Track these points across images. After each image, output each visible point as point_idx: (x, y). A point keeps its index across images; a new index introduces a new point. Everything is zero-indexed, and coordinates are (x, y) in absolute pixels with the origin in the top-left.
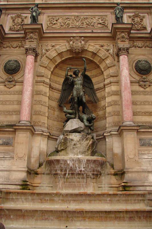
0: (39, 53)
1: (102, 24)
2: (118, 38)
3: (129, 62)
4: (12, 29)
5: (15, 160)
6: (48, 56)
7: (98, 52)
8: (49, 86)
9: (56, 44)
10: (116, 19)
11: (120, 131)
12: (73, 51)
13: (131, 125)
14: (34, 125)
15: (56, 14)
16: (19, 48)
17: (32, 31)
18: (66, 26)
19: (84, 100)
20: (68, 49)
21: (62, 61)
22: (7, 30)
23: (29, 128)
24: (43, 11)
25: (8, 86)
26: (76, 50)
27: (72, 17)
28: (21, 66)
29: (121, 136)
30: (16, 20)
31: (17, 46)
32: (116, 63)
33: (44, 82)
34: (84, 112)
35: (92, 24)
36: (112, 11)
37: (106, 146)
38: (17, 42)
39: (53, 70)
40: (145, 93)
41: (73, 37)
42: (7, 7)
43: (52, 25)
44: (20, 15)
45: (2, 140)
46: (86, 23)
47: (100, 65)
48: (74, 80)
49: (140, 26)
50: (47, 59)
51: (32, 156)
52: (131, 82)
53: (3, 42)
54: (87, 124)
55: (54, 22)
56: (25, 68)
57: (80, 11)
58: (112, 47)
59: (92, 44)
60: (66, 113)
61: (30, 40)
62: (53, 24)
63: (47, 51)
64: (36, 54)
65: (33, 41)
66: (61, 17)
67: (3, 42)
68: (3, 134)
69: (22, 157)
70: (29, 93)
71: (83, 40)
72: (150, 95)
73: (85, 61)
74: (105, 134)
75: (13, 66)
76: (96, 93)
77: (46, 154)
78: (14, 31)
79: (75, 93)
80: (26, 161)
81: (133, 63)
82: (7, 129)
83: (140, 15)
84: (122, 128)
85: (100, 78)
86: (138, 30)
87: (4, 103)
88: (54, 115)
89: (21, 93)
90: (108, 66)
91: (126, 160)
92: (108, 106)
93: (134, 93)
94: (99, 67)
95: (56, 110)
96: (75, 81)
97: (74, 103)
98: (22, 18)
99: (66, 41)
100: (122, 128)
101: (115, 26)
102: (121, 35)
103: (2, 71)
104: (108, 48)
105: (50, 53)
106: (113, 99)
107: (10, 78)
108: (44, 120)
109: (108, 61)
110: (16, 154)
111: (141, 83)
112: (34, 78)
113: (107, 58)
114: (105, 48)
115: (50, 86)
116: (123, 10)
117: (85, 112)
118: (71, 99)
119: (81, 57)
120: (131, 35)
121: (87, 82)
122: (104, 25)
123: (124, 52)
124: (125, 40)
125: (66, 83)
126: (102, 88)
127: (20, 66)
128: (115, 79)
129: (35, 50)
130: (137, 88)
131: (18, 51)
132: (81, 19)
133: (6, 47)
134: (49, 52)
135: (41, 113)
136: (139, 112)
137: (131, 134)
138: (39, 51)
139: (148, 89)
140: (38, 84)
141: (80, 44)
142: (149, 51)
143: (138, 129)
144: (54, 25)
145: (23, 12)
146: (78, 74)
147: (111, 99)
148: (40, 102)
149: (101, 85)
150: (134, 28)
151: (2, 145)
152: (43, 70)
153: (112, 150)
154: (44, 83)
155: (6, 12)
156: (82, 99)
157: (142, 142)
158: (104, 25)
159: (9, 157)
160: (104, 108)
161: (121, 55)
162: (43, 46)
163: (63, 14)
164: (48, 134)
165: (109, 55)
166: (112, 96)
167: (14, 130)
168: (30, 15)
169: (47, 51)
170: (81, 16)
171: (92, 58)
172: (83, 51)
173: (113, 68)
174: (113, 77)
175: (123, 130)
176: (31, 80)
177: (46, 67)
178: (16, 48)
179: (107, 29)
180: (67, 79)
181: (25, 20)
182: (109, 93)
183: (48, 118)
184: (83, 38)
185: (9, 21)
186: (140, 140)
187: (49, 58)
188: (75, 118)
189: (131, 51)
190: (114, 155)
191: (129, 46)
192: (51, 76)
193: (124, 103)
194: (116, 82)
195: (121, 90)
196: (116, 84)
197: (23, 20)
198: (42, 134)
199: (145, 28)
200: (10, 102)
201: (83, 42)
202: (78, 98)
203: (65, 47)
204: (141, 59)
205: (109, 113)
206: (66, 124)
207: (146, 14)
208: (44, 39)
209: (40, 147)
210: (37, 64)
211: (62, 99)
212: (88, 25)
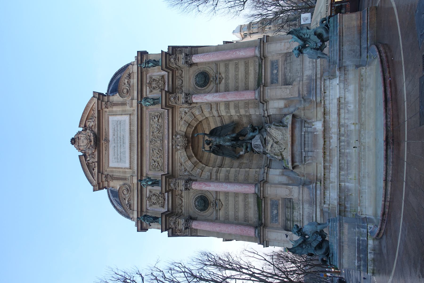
0: (189, 178)
1: (158, 118)
2: (176, 103)
3: (196, 93)
4: (163, 205)
5: (292, 197)
6: (191, 169)
7: (187, 122)
8: (220, 168)
9: (179, 162)
10: (154, 105)
11: (264, 102)
12: (186, 146)
13: (259, 92)
14: (258, 181)
15: (148, 162)
16: (182, 197)
17: (168, 184)
18: (161, 152)
19: (234, 135)
20: (184, 150)
21: (195, 156)
22: (165, 210)
23: (262, 185)
24: (144, 176)
25: (220, 207)
26: (185, 143)
27: (151, 147)
28: (201, 195)
29: (268, 101)
30: (153, 201)
31: (181, 199)
32: (198, 105)
33: (217, 172)
34: (245, 136)
35: (159, 127)
36: (144, 109)
37: (277, 114)
38: (176, 199)
39: (204, 164)
40: (227, 78)
42: (140, 211)
43: (159, 166)
44: (149, 197)
45: (273, 211)
46: (158, 134)
47: (200, 120)
48: (214, 144)
49: (160, 82)
50: (194, 170)
51: (287, 182)
52: (216, 91)
53: (176, 213)
54: (257, 132)
55: (157, 164)
56: (203, 190)
57: (144, 139)
58: (182, 109)
59: (179, 128)
60: (246, 151)
61: (177, 186)
62: (158, 165)
63: (186, 170)
64: (190, 180)
65: (178, 183)
66: (151, 157)
67: (176, 213)
68: (267, 209)
69: (290, 191)
70: (229, 185)
71: (176, 136)
72: (229, 74)
73: (198, 135)
74: (266, 115)
75: (201, 202)
76: (225, 125)
78: (165, 202)
79: (228, 144)
80: (293, 186)
81: (198, 89)
82: (263, 205)
83: (149, 82)
84: (262, 101)
85: (211, 120)
86: (164, 84)
87: (236, 210)
88: (247, 163)
89: (227, 194)
90: (201, 112)
91: (292, 96)
92: (239, 113)
93: (227, 89)
94: (201, 122)
95: (242, 161)
96: (216, 143)
97: (237, 144)
98: (151, 196)
99: (176, 153)
100: (262, 101)
101: (164, 107)
102: (173, 100)
103: (205, 214)
104: (183, 113)
105: (188, 167)
106: (233, 109)
107: (213, 205)
108: (252, 172)
109: (197, 112)
110: (286, 196)
111: (218, 81)
112: (213, 182)
113: (194, 114)
114: (183, 116)
115: (219, 167)
116: (145, 98)
117: (245, 134)
118: (233, 147)
119: (191, 138)
120: (171, 91)
121: (216, 133)
122: (160, 116)
123: (189, 98)
124: (177, 97)
125: (216, 152)
126: (221, 119)
127: (201, 196)
128: (214, 106)
129: (187, 181)
130: (222, 86)
131: (186, 198)
132: (154, 139)
133: (182, 210)
134: (186, 168)
135: (247, 174)
136: (245, 84)
137: (268, 92)
138: (187, 178)
139: (223, 76)
140: (218, 178)
141: (179, 139)
142: (186, 73)
143: (263, 86)
144: (159, 164)
145: (144, 195)
146: (209, 140)
147: (233, 110)
148: (236, 176)
149: (218, 119)
150: (163, 87)
151: (278, 211)
152: (206, 174)
153: (281, 109)
154: (217, 173)
155: (144, 211)
156: (233, 137)
157: (274, 82)
158: (159, 116)
159: (289, 204)
160: (240, 116)
161: (192, 101)
163: (148, 156)
164: (266, 168)
165: (190, 112)
166: (230, 109)
167: (264, 198)
168: (149, 188)
169: (186, 170)
170: (151, 139)
171: (192, 127)
172: (186, 136)
173: (202, 108)
174: (212, 108)
175: (264, 99)
176: (216, 184)
177: (202, 171)
178: (182, 201)
179: (164, 113)
180: (213, 152)
181: (153, 193)
182: (227, 112)
183: (250, 169)
184: (174, 137)
185: (154, 208)
186: (272, 83)
187: (193, 168)
188: (251, 143)
189: (186, 91)
190: (286, 107)
191: (183, 93)
192: (209, 166)
193: (238, 99)
194: (216, 105)
195: (225, 101)
196: (218, 106)
197: (154, 195)
198: (267, 173)
199: (162, 77)
200: (236, 204)
201: (178, 136)
202: (232, 140)
203: (182, 154)
204: (194, 81)
205: (246, 112)
206: (257, 151)
207: (148, 75)
208: (174, 174)
210: (199, 179)
211: (231, 156)
212: (160, 131)
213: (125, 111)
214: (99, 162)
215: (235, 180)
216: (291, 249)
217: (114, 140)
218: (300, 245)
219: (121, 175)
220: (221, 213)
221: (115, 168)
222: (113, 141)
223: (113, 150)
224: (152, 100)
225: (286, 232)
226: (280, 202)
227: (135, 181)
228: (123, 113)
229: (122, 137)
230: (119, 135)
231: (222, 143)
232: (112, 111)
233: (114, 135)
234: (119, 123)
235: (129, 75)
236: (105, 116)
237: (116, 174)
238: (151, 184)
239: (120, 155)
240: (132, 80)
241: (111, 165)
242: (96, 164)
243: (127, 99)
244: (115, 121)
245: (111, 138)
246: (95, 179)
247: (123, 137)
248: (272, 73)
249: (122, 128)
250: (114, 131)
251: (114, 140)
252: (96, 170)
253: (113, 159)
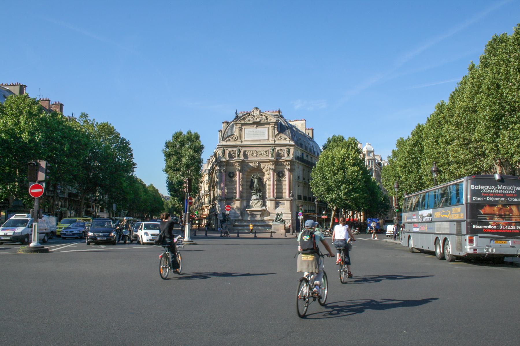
41: (254, 162)
63: (244, 167)
114: (266, 166)
214: (246, 123)
220: (228, 183)
227: (239, 143)
229: (258, 135)
231: (255, 183)
235: (285, 139)
236: (267, 126)
242: (245, 122)
245: (257, 129)
250: (261, 131)
252: (242, 122)
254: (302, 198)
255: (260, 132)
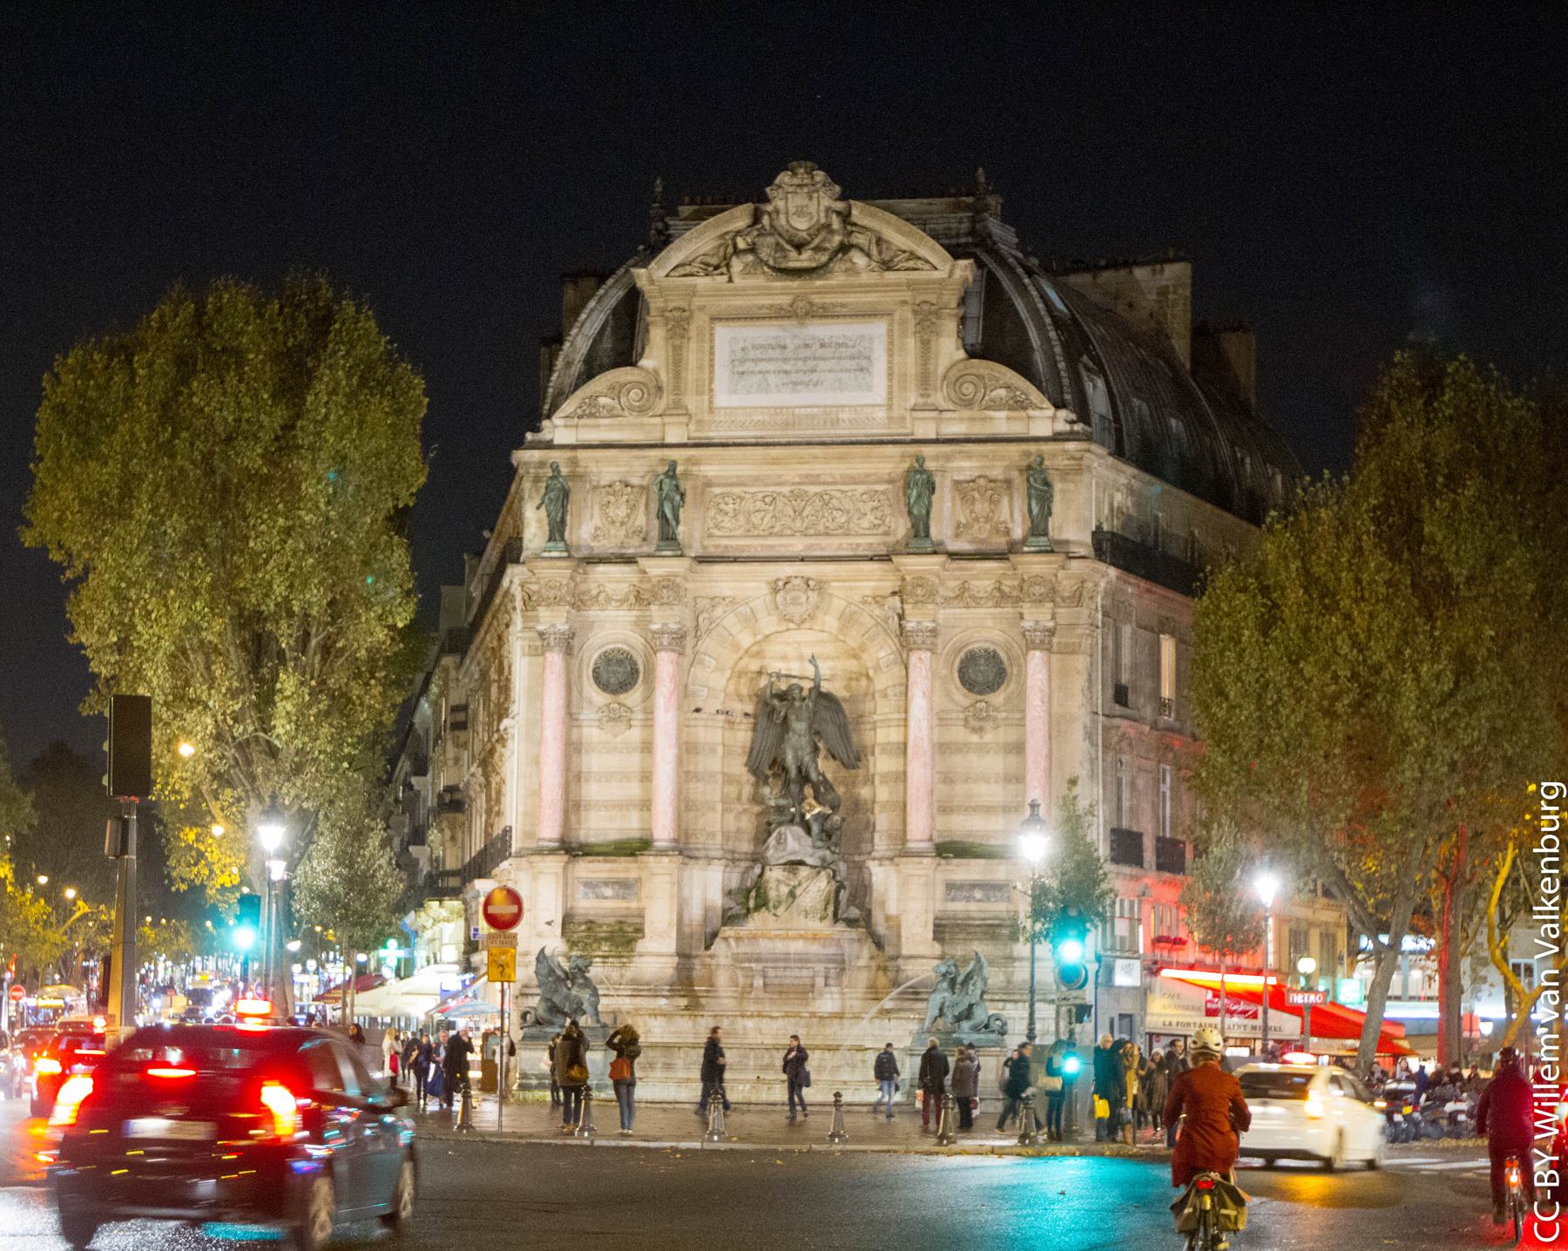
19: (813, 776)
40: (982, 749)
77: (720, 913)
130: (959, 734)
139: (989, 737)
153: (883, 904)
162: (699, 600)
176: (672, 727)
202: (799, 769)
209: (705, 900)
213: (903, 388)
215: (687, 773)
216: (545, 957)
217: (807, 346)
218: (551, 972)
219: (690, 375)
221: (712, 353)
222: (800, 342)
223: (773, 342)
224: (924, 512)
225: (559, 921)
226: (634, 905)
228: (895, 381)
230: (822, 365)
232: (904, 335)
233: (822, 346)
234: (864, 363)
237: (692, 358)
238: (663, 512)
239: (756, 369)
240: (1003, 414)
241: (722, 332)
243: (939, 398)
244: (871, 350)
246: (673, 274)
247: (816, 384)
248: (974, 886)
249: (844, 376)
250: (840, 345)
251: (807, 346)
253: (741, 345)
254: (1149, 855)
255: (827, 352)
